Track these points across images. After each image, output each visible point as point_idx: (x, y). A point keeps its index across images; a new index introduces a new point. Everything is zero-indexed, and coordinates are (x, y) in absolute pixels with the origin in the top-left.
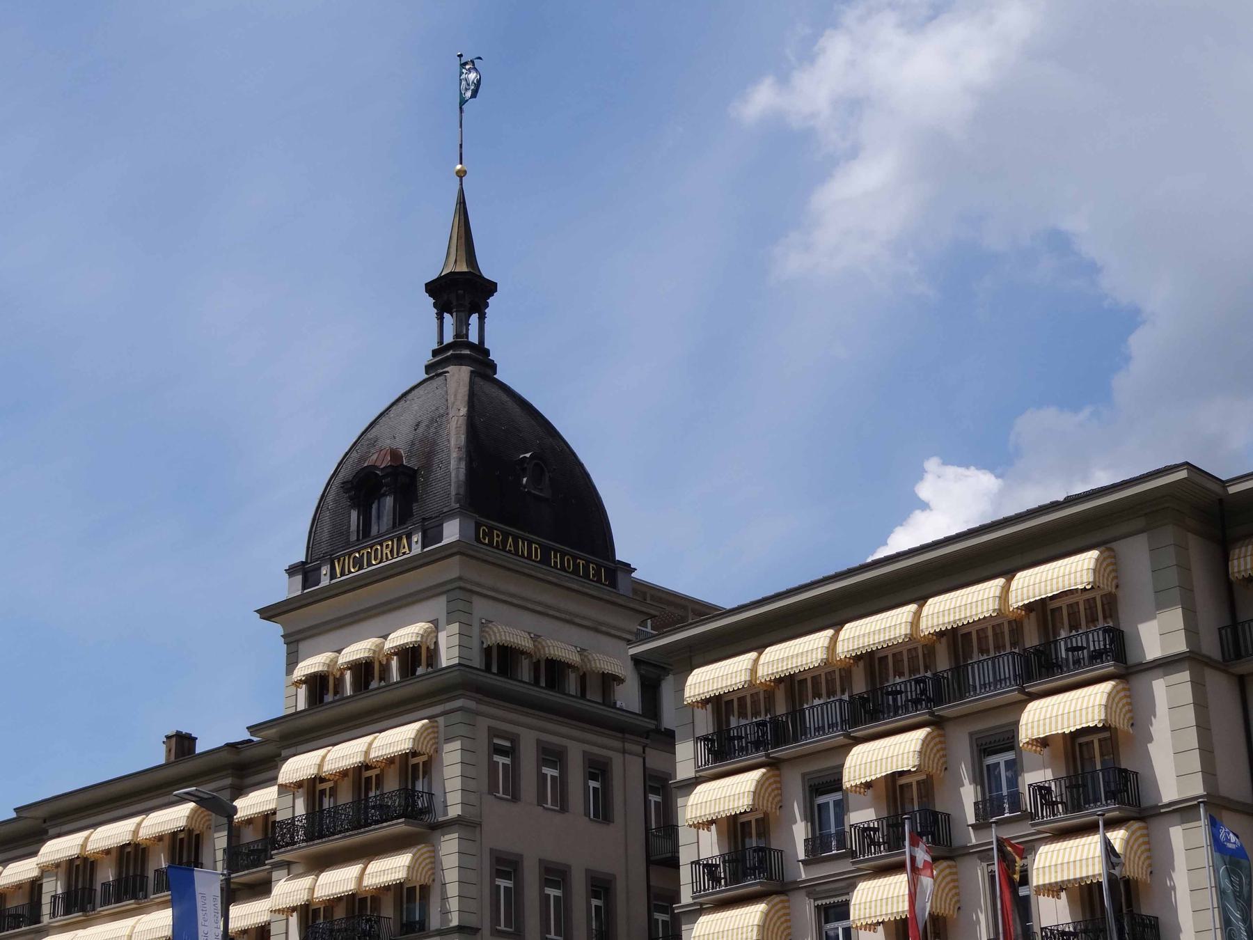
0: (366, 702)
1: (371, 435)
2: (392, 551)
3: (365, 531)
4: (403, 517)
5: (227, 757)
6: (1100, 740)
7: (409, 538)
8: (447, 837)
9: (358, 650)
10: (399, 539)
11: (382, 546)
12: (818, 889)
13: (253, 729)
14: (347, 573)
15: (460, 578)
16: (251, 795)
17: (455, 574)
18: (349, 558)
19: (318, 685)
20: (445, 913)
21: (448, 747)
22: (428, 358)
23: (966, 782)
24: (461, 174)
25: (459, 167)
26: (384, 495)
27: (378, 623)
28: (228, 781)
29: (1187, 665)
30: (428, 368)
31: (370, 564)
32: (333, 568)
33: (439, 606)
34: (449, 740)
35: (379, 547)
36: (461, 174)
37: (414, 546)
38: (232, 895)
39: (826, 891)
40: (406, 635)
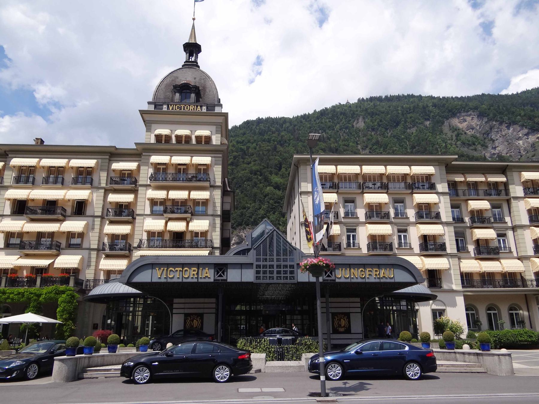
0: (199, 147)
1: (174, 75)
2: (194, 109)
3: (182, 100)
4: (198, 100)
5: (113, 150)
6: (424, 206)
7: (201, 107)
8: (216, 190)
9: (183, 132)
10: (197, 106)
11: (190, 106)
12: (347, 224)
13: (136, 144)
14: (174, 109)
15: (222, 123)
16: (120, 163)
17: (221, 121)
18: (176, 105)
19: (159, 138)
20: (215, 210)
21: (215, 166)
22: (183, 63)
23: (391, 208)
24: (194, 19)
25: (194, 17)
26: (191, 93)
27: (173, 127)
28: (108, 157)
29: (448, 195)
30: (183, 66)
31: (184, 109)
32: (168, 107)
33: (214, 128)
34: (216, 164)
35: (189, 107)
36: (194, 19)
37: (203, 109)
38: (107, 191)
39: (402, 225)
40: (204, 132)
